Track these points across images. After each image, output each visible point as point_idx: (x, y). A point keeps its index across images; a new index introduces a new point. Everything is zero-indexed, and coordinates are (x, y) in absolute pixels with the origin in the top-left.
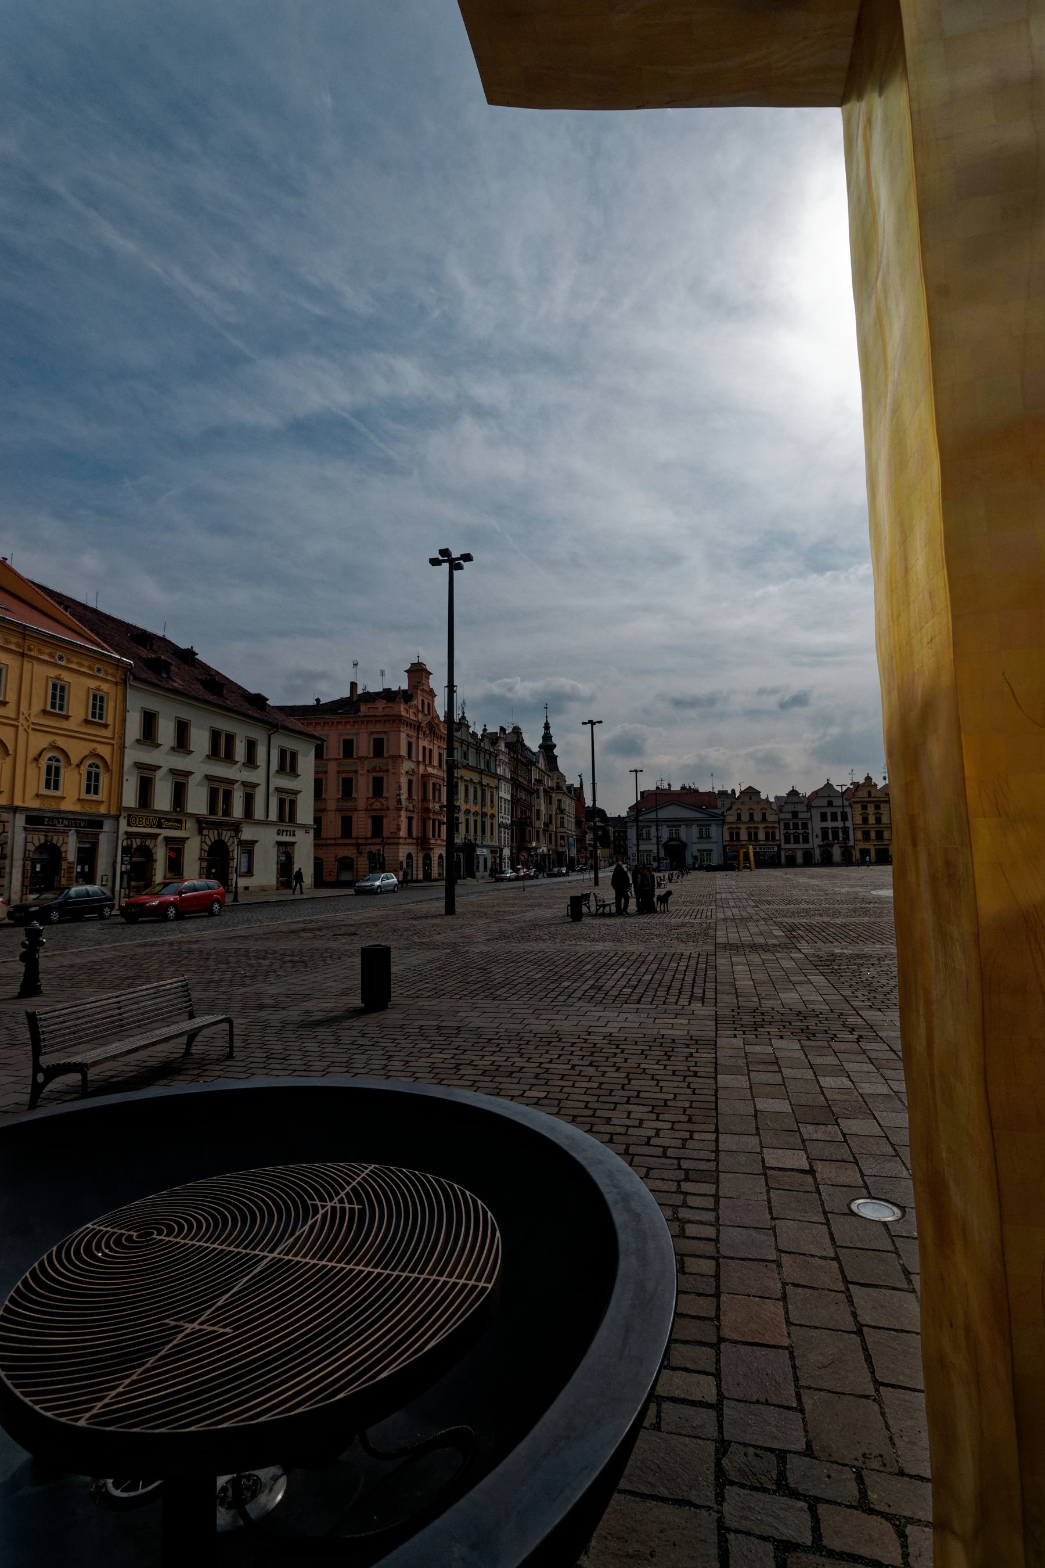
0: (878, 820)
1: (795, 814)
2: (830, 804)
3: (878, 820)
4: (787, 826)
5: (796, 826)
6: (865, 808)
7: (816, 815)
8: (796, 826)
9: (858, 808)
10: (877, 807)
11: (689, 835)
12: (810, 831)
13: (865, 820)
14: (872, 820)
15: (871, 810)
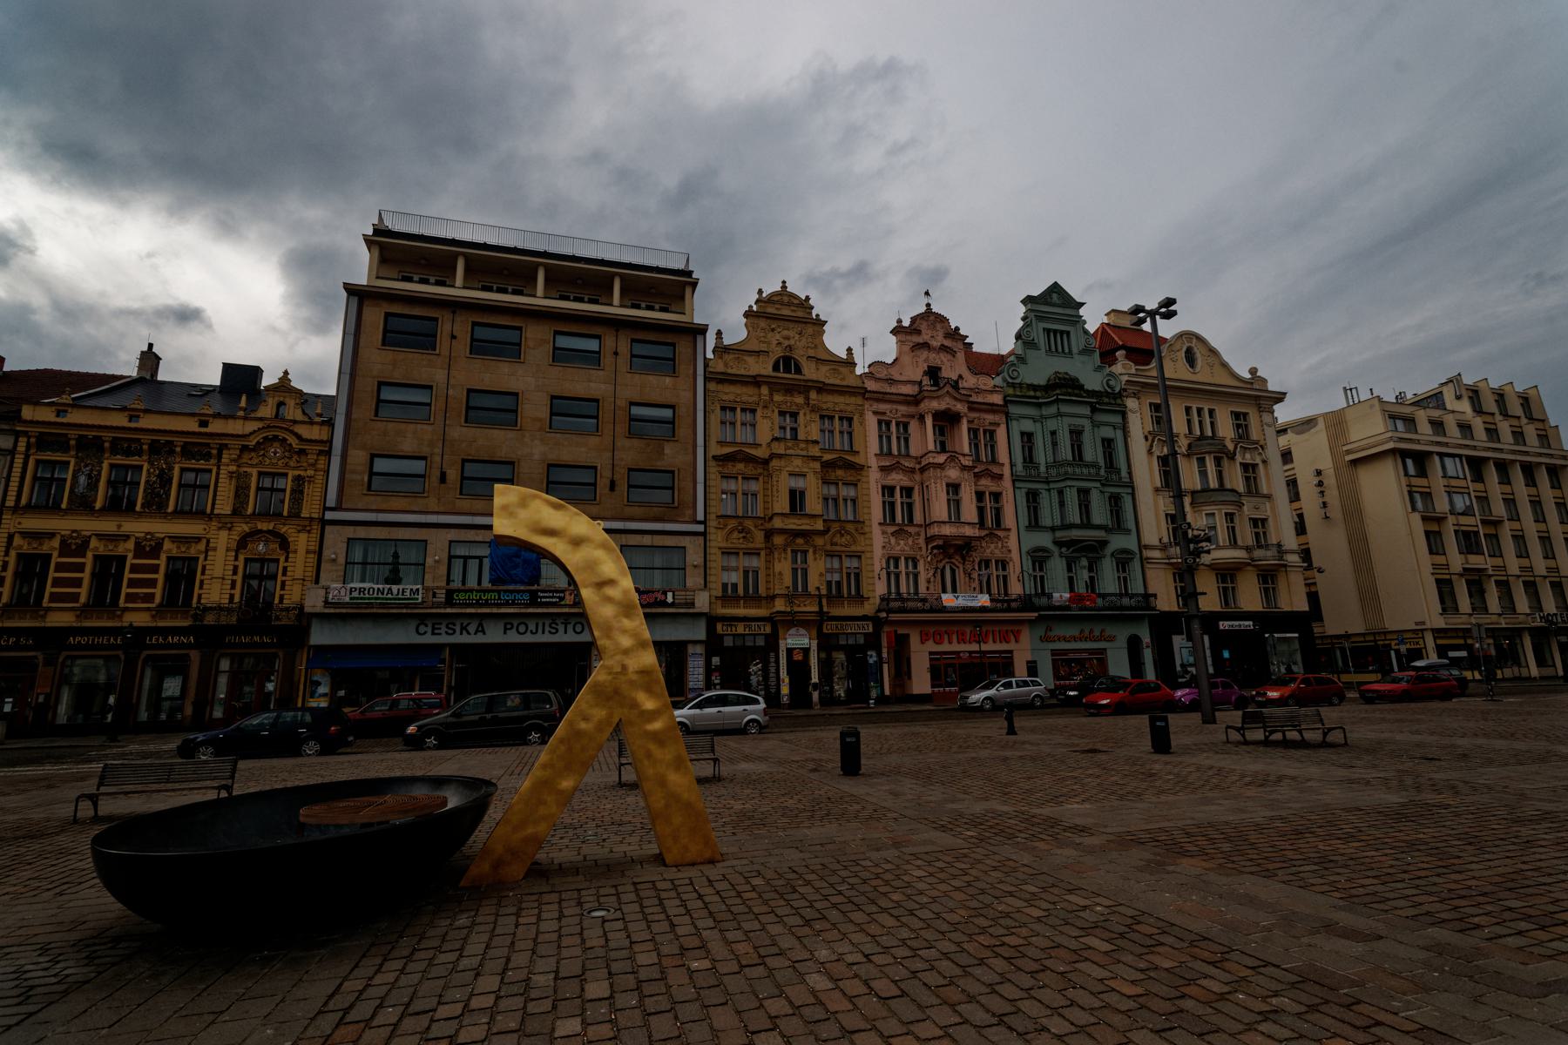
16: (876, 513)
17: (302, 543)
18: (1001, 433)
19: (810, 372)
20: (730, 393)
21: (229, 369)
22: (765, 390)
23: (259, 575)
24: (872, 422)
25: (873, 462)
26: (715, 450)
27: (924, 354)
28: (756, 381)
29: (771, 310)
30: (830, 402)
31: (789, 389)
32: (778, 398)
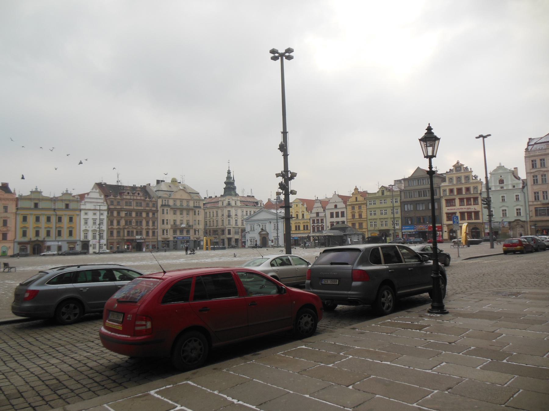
0: (360, 216)
1: (318, 214)
2: (336, 206)
3: (360, 216)
4: (314, 221)
5: (318, 220)
6: (353, 208)
7: (328, 214)
8: (318, 220)
9: (349, 208)
10: (360, 208)
11: (270, 228)
12: (324, 224)
13: (353, 216)
14: (357, 216)
15: (357, 208)
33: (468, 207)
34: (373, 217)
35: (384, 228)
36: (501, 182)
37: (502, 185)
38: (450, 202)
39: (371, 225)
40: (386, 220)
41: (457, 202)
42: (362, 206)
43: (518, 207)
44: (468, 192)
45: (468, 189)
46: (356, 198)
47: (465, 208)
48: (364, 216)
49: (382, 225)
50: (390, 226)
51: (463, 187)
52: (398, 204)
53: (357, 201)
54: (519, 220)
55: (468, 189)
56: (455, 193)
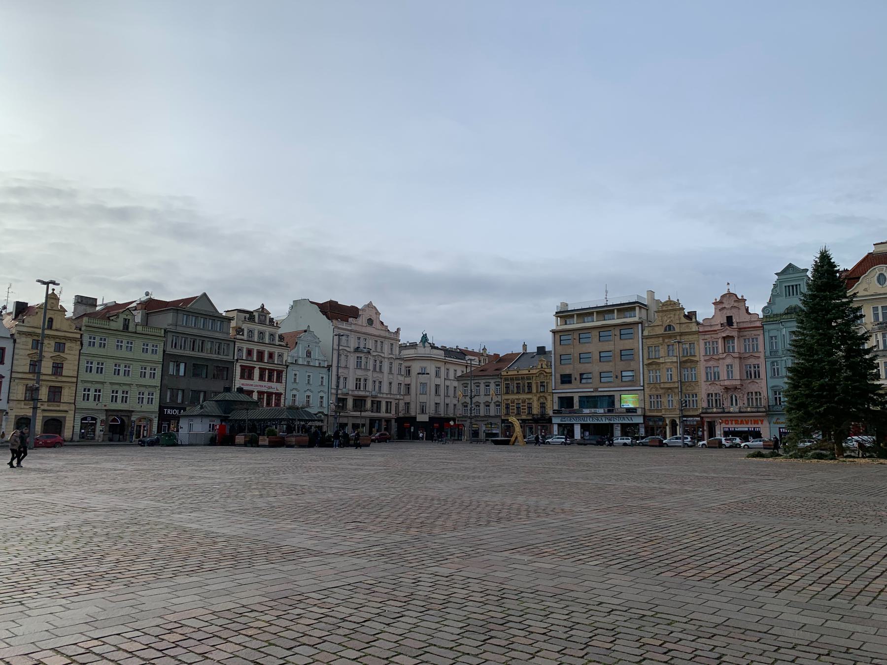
0: (58, 368)
3: (58, 368)
10: (60, 347)
13: (35, 365)
14: (47, 367)
15: (49, 348)
16: (704, 378)
17: (549, 398)
18: (761, 338)
19: (677, 330)
20: (650, 342)
21: (538, 348)
22: (661, 339)
23: (543, 406)
24: (702, 343)
25: (702, 359)
26: (646, 362)
27: (725, 311)
28: (657, 336)
29: (664, 308)
30: (685, 338)
31: (670, 337)
32: (666, 341)
33: (270, 384)
34: (94, 376)
35: (119, 405)
36: (309, 354)
37: (308, 359)
38: (247, 373)
39: (86, 398)
40: (126, 388)
41: (257, 373)
42: (68, 345)
43: (322, 394)
44: (271, 361)
45: (271, 355)
46: (51, 320)
47: (265, 386)
48: (69, 369)
49: (114, 399)
50: (132, 404)
51: (267, 350)
52: (159, 357)
53: (50, 327)
54: (322, 413)
55: (271, 355)
56: (255, 359)
